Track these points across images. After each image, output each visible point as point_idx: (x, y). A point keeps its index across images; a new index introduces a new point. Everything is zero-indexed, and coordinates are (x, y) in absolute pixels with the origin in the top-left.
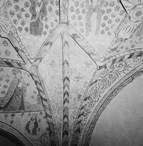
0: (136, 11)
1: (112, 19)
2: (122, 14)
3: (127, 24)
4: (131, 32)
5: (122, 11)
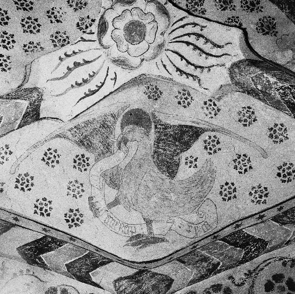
0: (128, 13)
1: (43, 20)
2: (84, 27)
3: (82, 46)
4: (87, 95)
5: (88, 17)
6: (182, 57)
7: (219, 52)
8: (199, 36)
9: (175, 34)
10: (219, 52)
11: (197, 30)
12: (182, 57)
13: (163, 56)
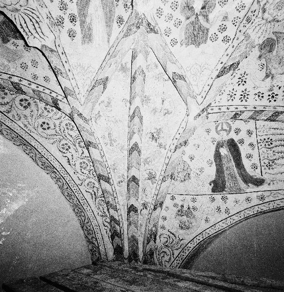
6: (25, 23)
7: (42, 36)
8: (37, 22)
9: (26, 11)
10: (42, 36)
11: (37, 19)
12: (25, 23)
13: (17, 15)
